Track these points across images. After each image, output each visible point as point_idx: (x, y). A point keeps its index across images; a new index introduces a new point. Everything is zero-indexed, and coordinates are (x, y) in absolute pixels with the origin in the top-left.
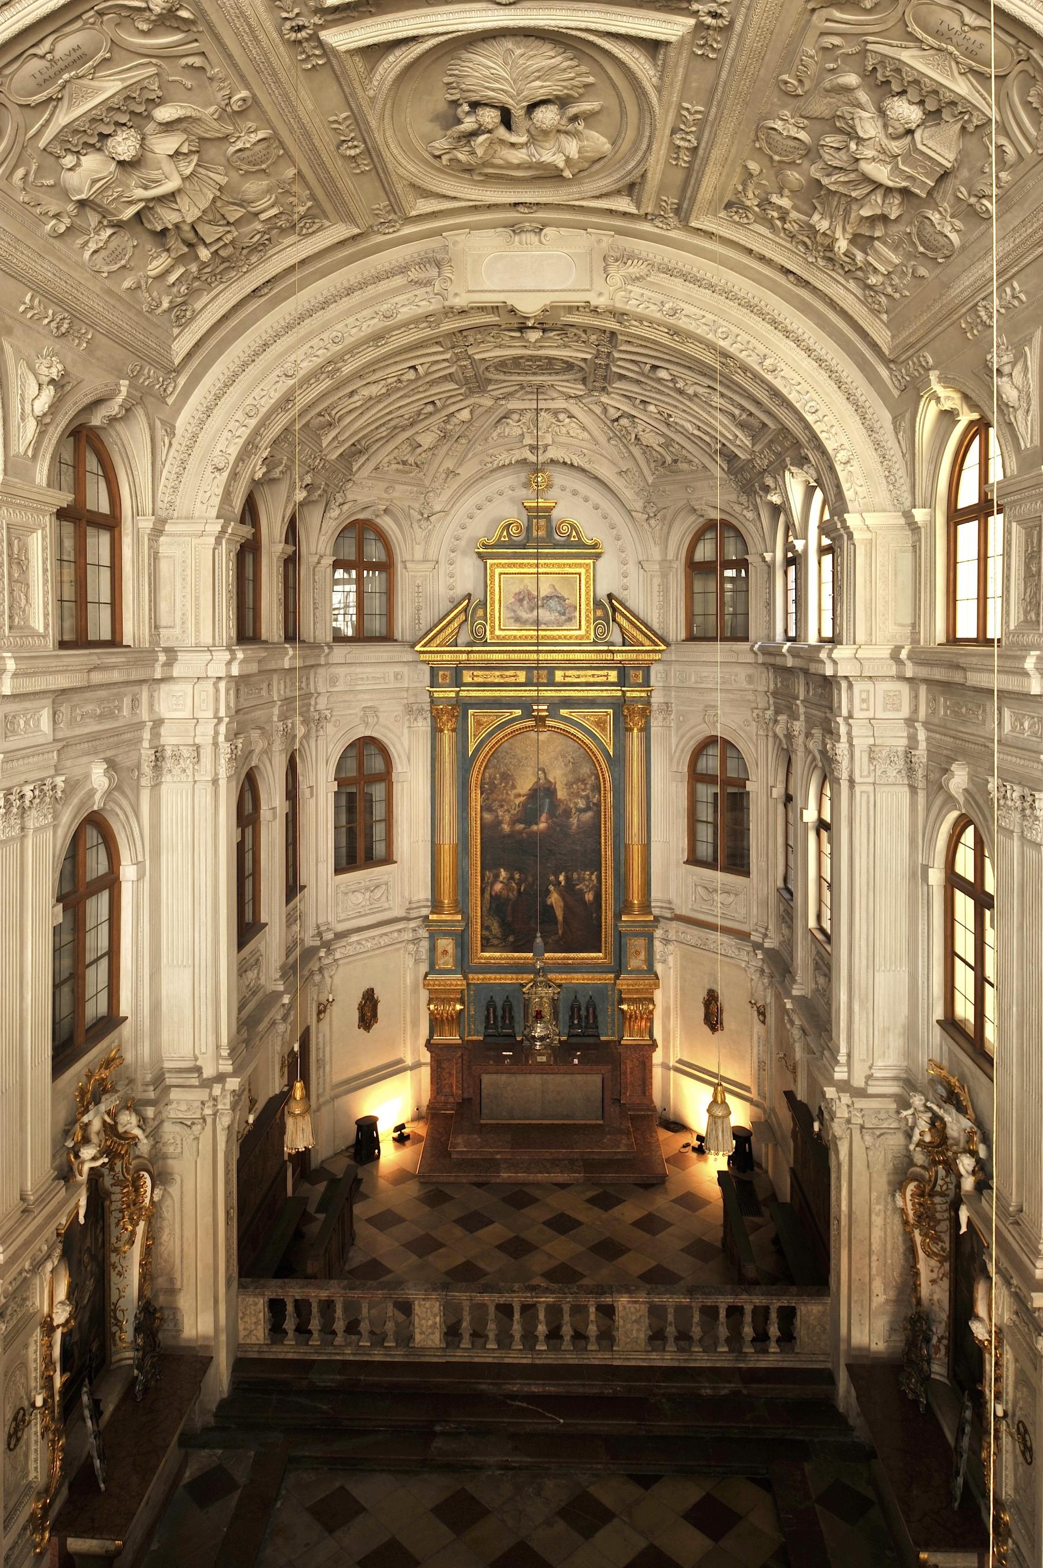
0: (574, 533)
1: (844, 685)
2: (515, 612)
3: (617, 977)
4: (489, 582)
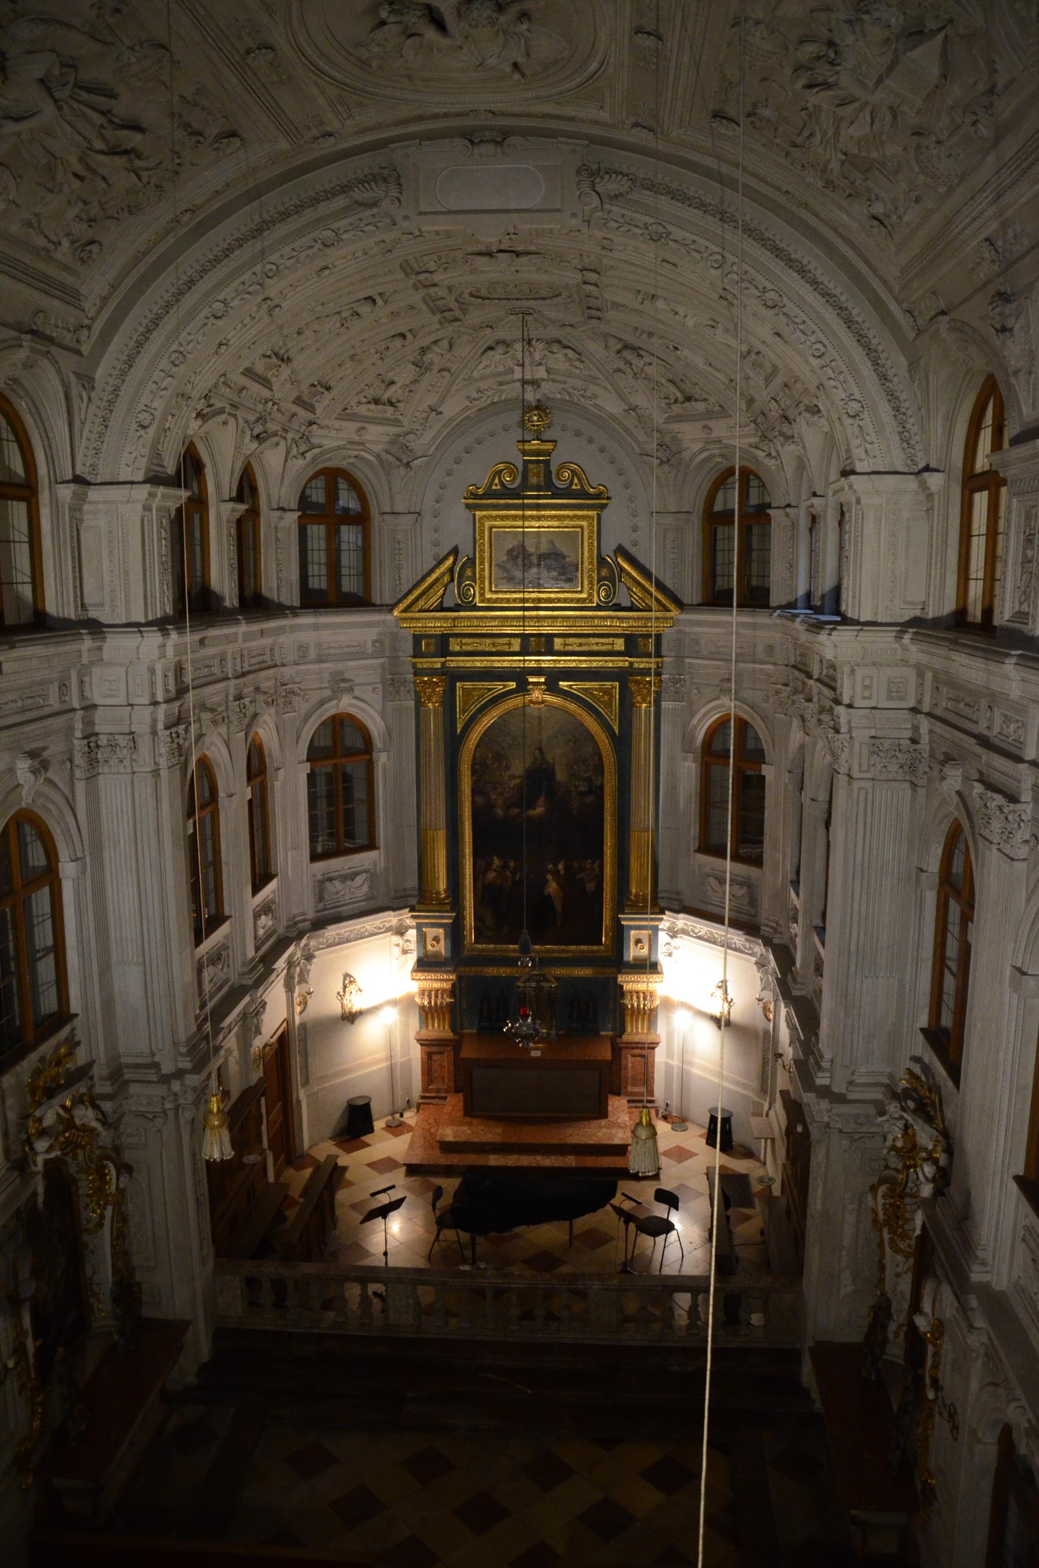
0: (576, 481)
2: (508, 571)
3: (620, 972)
4: (478, 537)
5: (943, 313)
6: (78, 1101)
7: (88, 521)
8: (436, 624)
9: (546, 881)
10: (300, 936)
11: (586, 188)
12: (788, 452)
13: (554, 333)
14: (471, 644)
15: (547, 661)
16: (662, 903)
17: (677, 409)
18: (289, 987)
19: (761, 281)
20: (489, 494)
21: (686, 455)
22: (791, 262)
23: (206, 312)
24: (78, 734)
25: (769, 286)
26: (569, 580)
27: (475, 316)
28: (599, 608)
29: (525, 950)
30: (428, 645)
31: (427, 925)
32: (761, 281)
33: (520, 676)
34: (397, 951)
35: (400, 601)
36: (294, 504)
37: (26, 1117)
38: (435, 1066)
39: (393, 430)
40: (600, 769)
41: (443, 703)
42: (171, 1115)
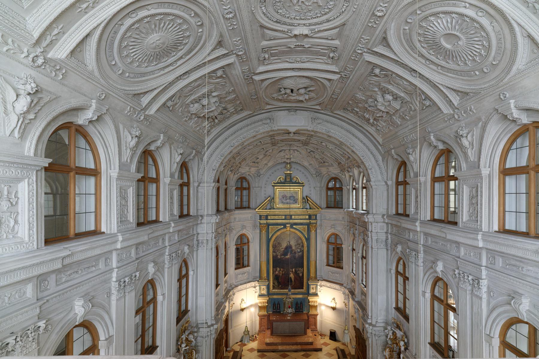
1: (370, 224)
5: (393, 149)
6: (190, 333)
7: (199, 190)
8: (264, 212)
9: (289, 274)
10: (233, 289)
11: (313, 122)
12: (347, 175)
13: (295, 148)
14: (273, 217)
15: (291, 221)
16: (318, 278)
17: (321, 164)
18: (229, 303)
19: (350, 141)
20: (278, 183)
21: (323, 175)
22: (356, 137)
23: (229, 145)
24: (195, 240)
25: (352, 142)
26: (296, 202)
27: (279, 145)
28: (303, 209)
29: (289, 291)
30: (263, 217)
31: (261, 285)
32: (350, 141)
33: (285, 225)
34: (254, 292)
35: (258, 207)
36: (234, 185)
37: (179, 338)
38: (263, 322)
39: (256, 169)
40: (303, 246)
41: (266, 231)
42: (209, 336)
